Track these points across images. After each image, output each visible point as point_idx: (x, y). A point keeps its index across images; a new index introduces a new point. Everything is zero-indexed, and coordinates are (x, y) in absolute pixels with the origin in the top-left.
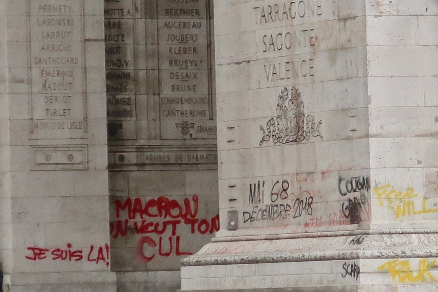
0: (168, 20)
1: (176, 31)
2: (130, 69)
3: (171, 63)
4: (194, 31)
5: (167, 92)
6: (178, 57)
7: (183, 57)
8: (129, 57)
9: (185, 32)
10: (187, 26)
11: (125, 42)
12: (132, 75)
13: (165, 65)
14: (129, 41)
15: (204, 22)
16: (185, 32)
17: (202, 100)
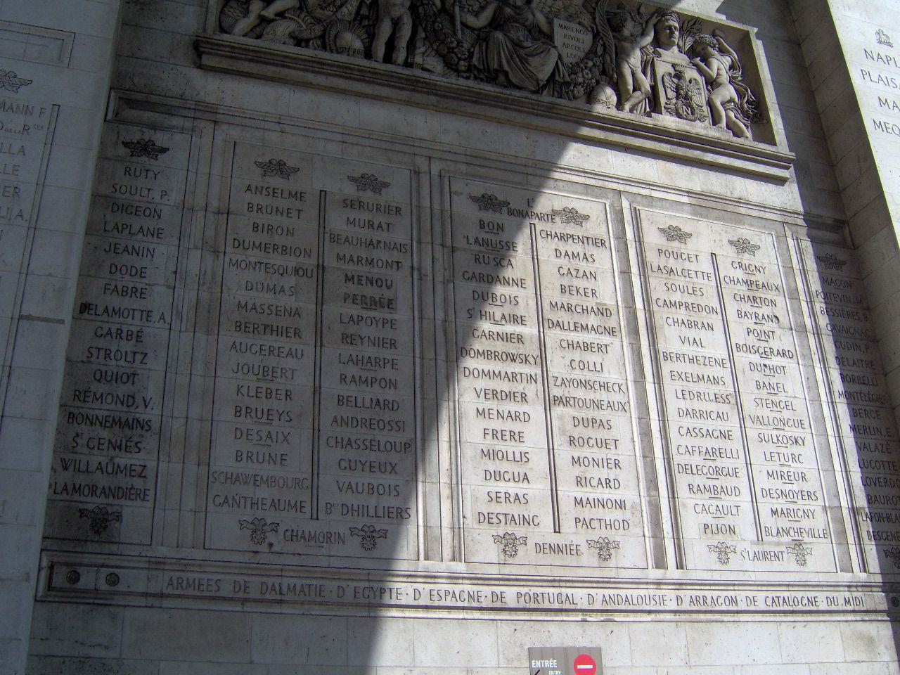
0: (238, 337)
1: (255, 360)
2: (152, 414)
3: (238, 412)
4: (289, 363)
5: (224, 460)
6: (254, 403)
7: (263, 404)
8: (153, 392)
9: (272, 361)
10: (276, 352)
11: (148, 366)
12: (155, 425)
13: (226, 414)
14: (155, 366)
15: (309, 350)
16: (272, 361)
17: (298, 483)
